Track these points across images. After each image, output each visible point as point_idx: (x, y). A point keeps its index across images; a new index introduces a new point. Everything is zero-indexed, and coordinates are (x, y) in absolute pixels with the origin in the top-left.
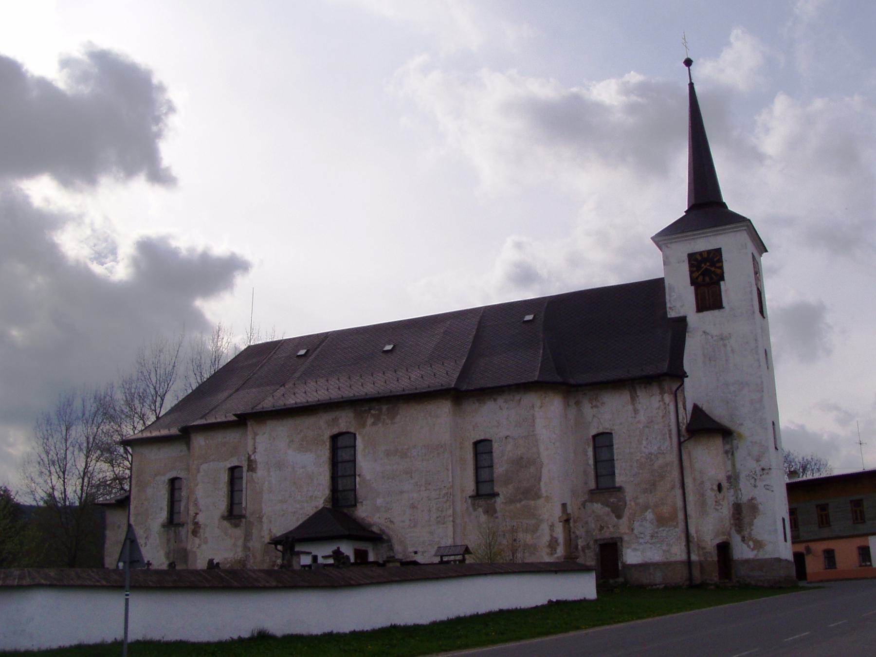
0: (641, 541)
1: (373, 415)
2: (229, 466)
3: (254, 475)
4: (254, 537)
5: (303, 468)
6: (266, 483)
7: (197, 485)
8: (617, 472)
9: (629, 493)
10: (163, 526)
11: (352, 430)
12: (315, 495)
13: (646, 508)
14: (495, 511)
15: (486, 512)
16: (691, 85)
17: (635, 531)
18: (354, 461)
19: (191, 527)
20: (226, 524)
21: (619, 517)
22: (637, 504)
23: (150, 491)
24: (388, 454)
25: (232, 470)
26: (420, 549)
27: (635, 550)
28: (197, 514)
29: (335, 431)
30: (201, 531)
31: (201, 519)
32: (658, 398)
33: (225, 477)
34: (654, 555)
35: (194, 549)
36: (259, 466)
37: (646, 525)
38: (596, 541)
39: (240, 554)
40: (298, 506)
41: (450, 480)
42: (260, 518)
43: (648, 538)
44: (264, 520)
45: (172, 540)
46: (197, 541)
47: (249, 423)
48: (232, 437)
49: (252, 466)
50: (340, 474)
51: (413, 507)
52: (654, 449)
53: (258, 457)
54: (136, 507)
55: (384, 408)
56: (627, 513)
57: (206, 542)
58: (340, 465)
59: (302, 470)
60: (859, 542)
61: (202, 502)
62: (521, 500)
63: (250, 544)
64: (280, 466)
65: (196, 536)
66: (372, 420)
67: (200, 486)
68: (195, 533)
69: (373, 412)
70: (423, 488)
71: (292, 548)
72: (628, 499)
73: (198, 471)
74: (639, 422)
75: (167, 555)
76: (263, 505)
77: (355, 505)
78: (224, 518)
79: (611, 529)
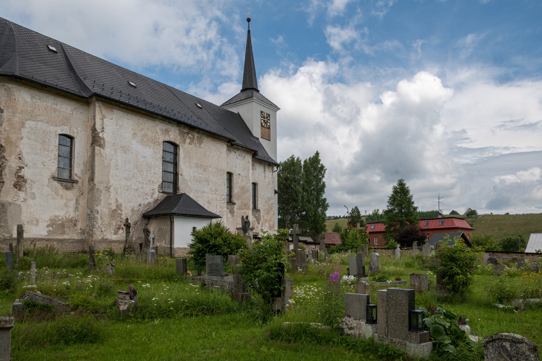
1: (190, 138)
4: (102, 203)
5: (144, 157)
6: (113, 161)
7: (22, 139)
13: (266, 221)
14: (234, 212)
16: (249, 31)
28: (21, 168)
30: (27, 186)
31: (25, 173)
32: (271, 173)
35: (17, 202)
40: (139, 185)
42: (108, 189)
44: (111, 190)
46: (22, 195)
57: (33, 197)
59: (143, 159)
61: (27, 158)
64: (125, 150)
65: (20, 190)
67: (25, 140)
70: (214, 193)
72: (261, 216)
73: (23, 125)
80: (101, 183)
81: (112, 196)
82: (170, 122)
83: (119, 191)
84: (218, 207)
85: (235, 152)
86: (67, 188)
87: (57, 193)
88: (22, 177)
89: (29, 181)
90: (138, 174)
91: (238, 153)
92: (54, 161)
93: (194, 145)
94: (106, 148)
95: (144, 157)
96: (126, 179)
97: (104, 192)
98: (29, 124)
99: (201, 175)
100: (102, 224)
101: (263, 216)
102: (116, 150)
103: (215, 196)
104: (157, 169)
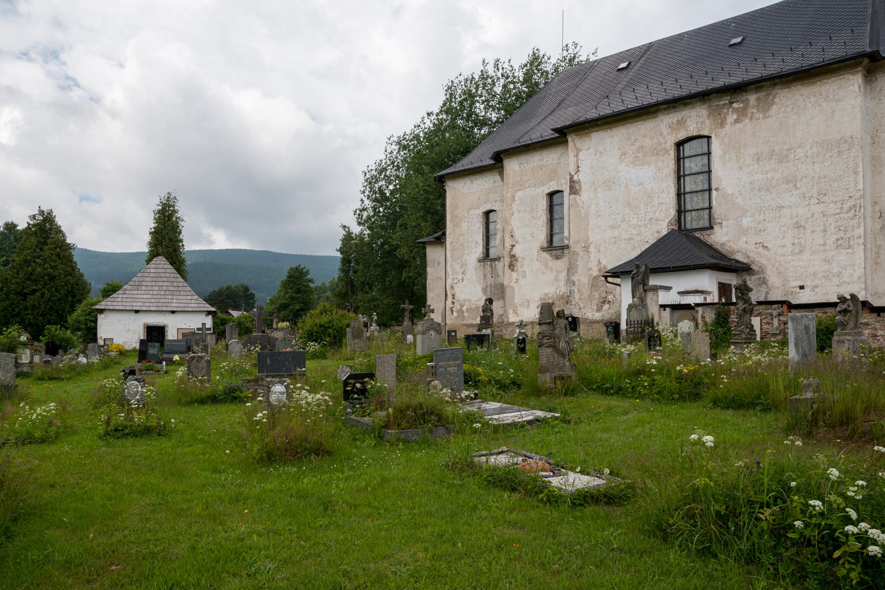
1: (736, 110)
3: (578, 197)
4: (579, 269)
5: (639, 185)
6: (593, 207)
10: (479, 261)
11: (706, 133)
19: (507, 260)
20: (545, 255)
23: (464, 226)
24: (758, 158)
25: (551, 195)
26: (808, 283)
28: (513, 246)
29: (682, 135)
30: (519, 264)
31: (517, 251)
33: (543, 204)
35: (512, 284)
36: (584, 187)
39: (563, 289)
41: (861, 187)
42: (586, 248)
44: (592, 249)
45: (489, 276)
46: (514, 275)
47: (570, 139)
48: (549, 158)
49: (574, 188)
51: (798, 226)
53: (582, 177)
54: (452, 242)
55: (752, 98)
57: (524, 277)
61: (517, 234)
63: (575, 278)
65: (513, 270)
66: (735, 117)
68: (512, 267)
69: (735, 105)
71: (644, 282)
75: (484, 290)
76: (590, 232)
77: (711, 228)
78: (543, 249)
80: (577, 242)
81: (592, 256)
82: (686, 105)
83: (602, 248)
84: (832, 229)
86: (557, 258)
87: (546, 267)
88: (514, 256)
89: (520, 259)
90: (632, 213)
92: (542, 228)
93: (747, 121)
94: (582, 193)
96: (612, 227)
97: (581, 254)
99: (769, 175)
100: (580, 299)
102: (596, 190)
103: (818, 209)
104: (665, 195)
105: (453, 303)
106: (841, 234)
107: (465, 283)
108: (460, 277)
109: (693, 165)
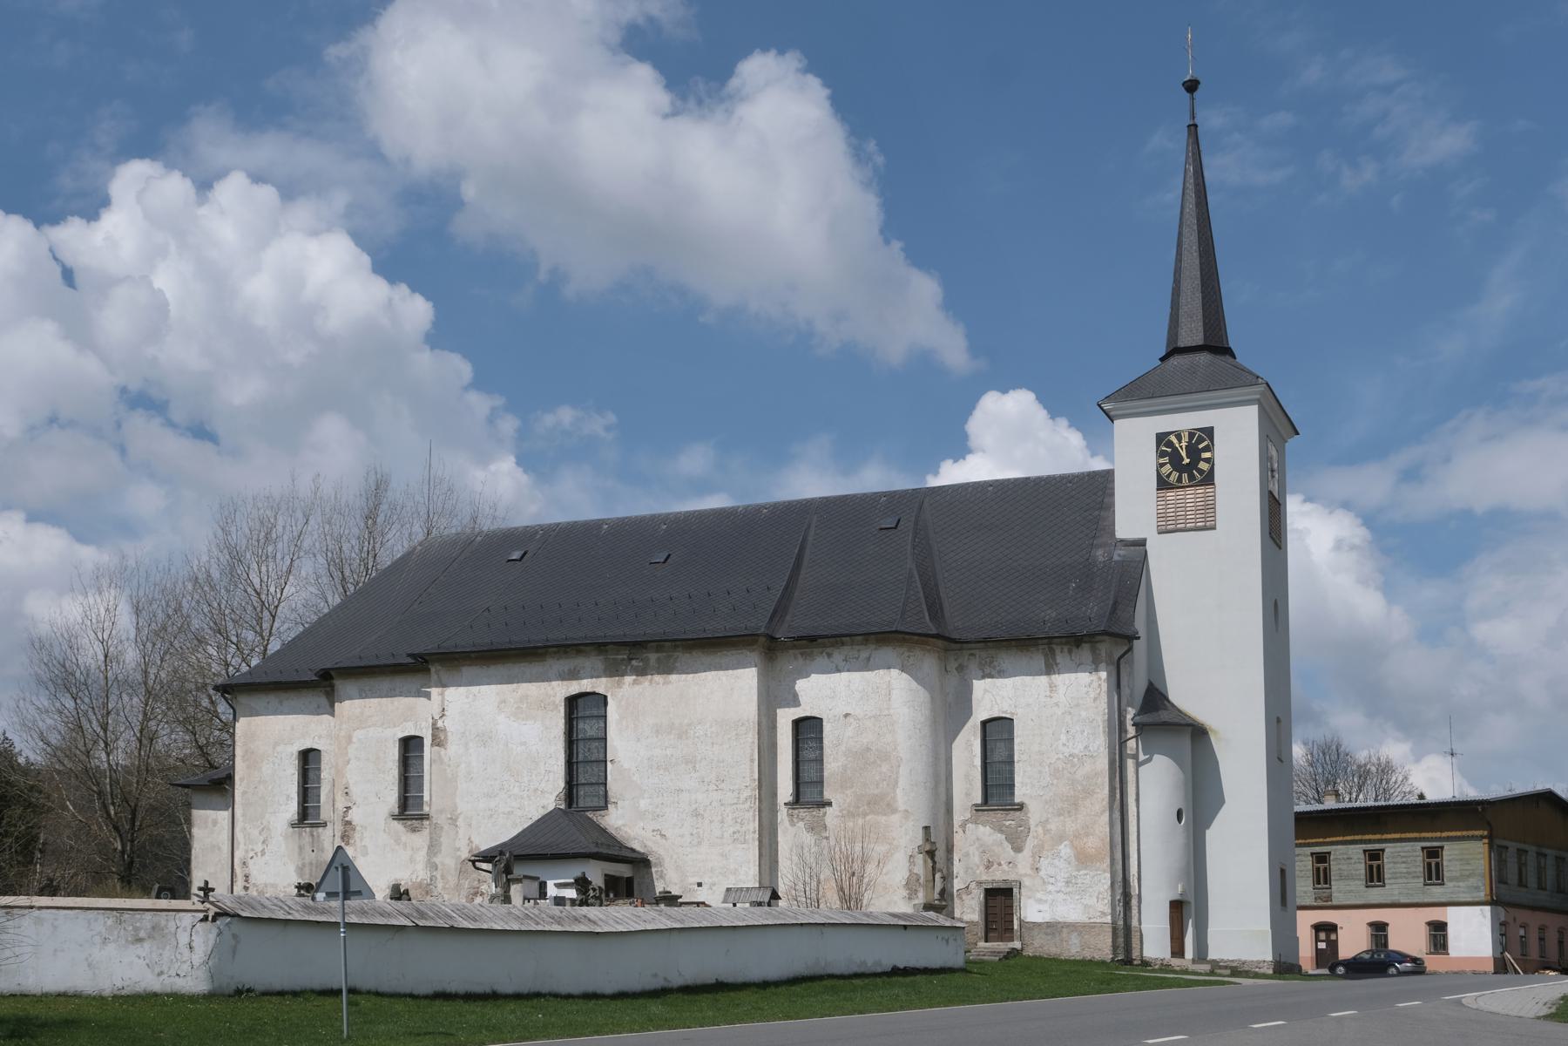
0: (1050, 888)
2: (401, 735)
3: (443, 752)
5: (523, 744)
8: (1018, 779)
9: (1035, 813)
10: (293, 826)
12: (542, 792)
13: (1061, 838)
15: (811, 829)
17: (1042, 873)
18: (604, 739)
19: (339, 828)
20: (398, 826)
21: (1018, 849)
22: (1046, 831)
27: (1040, 901)
30: (357, 835)
31: (353, 815)
33: (394, 753)
34: (1069, 910)
37: (1058, 864)
38: (980, 883)
42: (453, 821)
43: (1061, 884)
44: (460, 822)
49: (438, 739)
50: (581, 758)
51: (696, 814)
52: (1078, 748)
54: (244, 793)
56: (1030, 843)
58: (581, 744)
60: (1435, 914)
61: (354, 790)
62: (865, 815)
63: (437, 860)
71: (508, 870)
72: (1032, 823)
74: (1057, 705)
77: (606, 808)
79: (1005, 867)
80: (441, 812)
81: (461, 832)
85: (829, 655)
86: (414, 830)
87: (398, 841)
88: (349, 823)
91: (846, 650)
94: (448, 745)
95: (523, 744)
98: (358, 735)
99: (668, 752)
101: (1044, 823)
105: (246, 888)
106: (738, 827)
107: (267, 857)
108: (259, 848)
109: (587, 727)
